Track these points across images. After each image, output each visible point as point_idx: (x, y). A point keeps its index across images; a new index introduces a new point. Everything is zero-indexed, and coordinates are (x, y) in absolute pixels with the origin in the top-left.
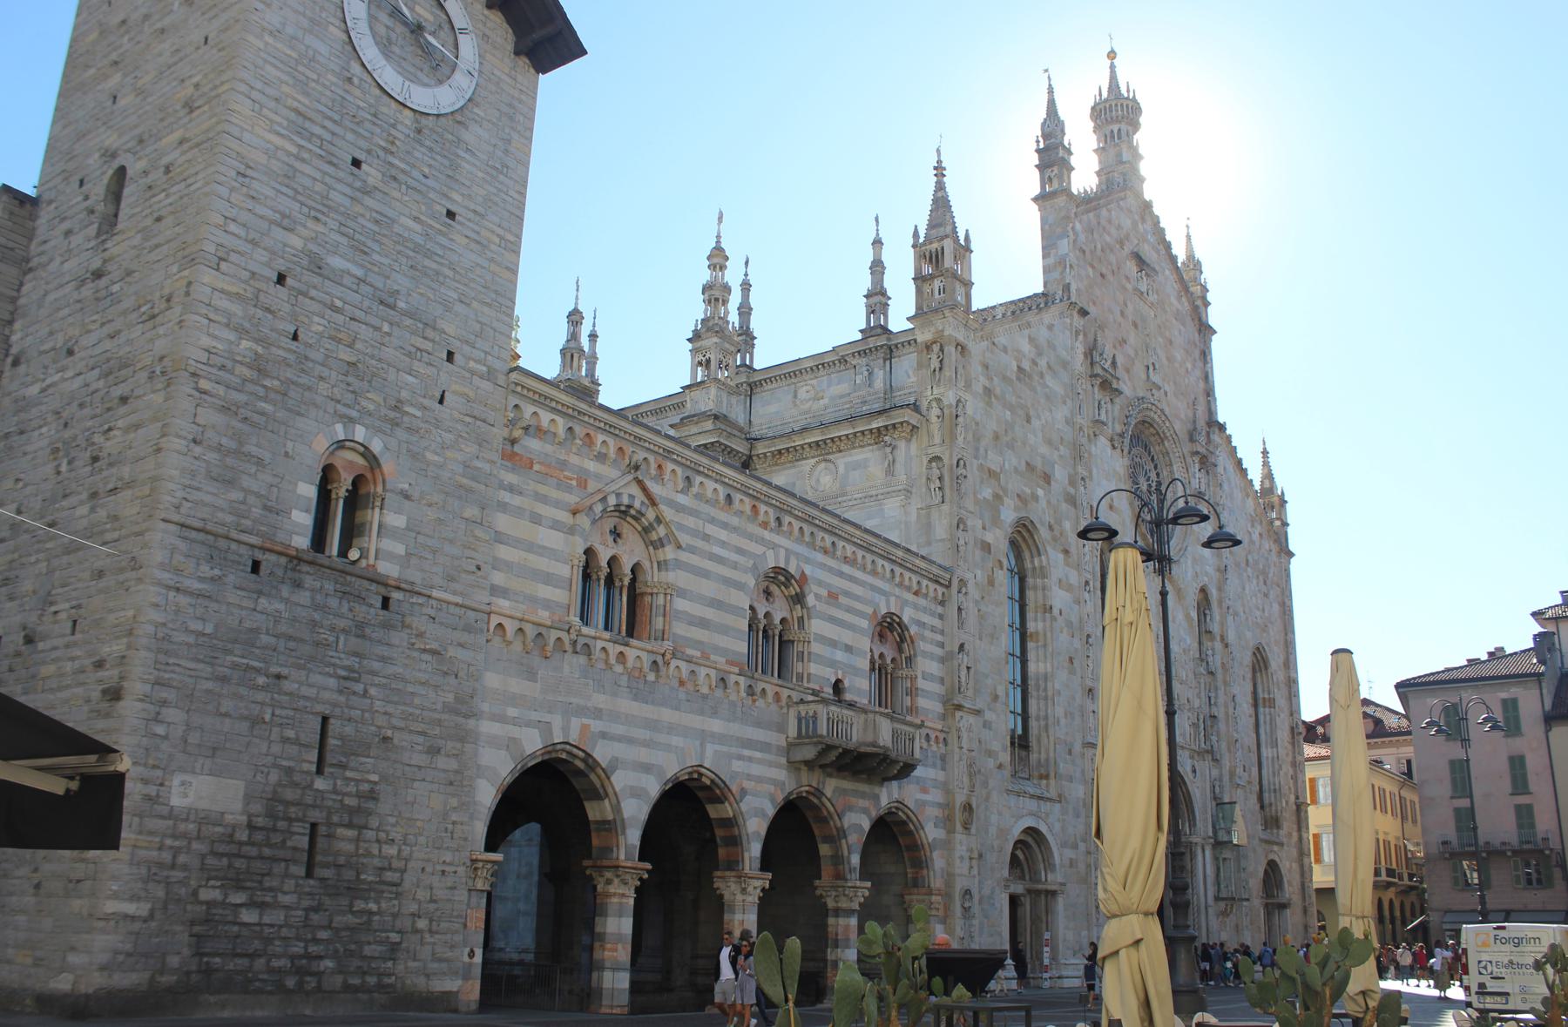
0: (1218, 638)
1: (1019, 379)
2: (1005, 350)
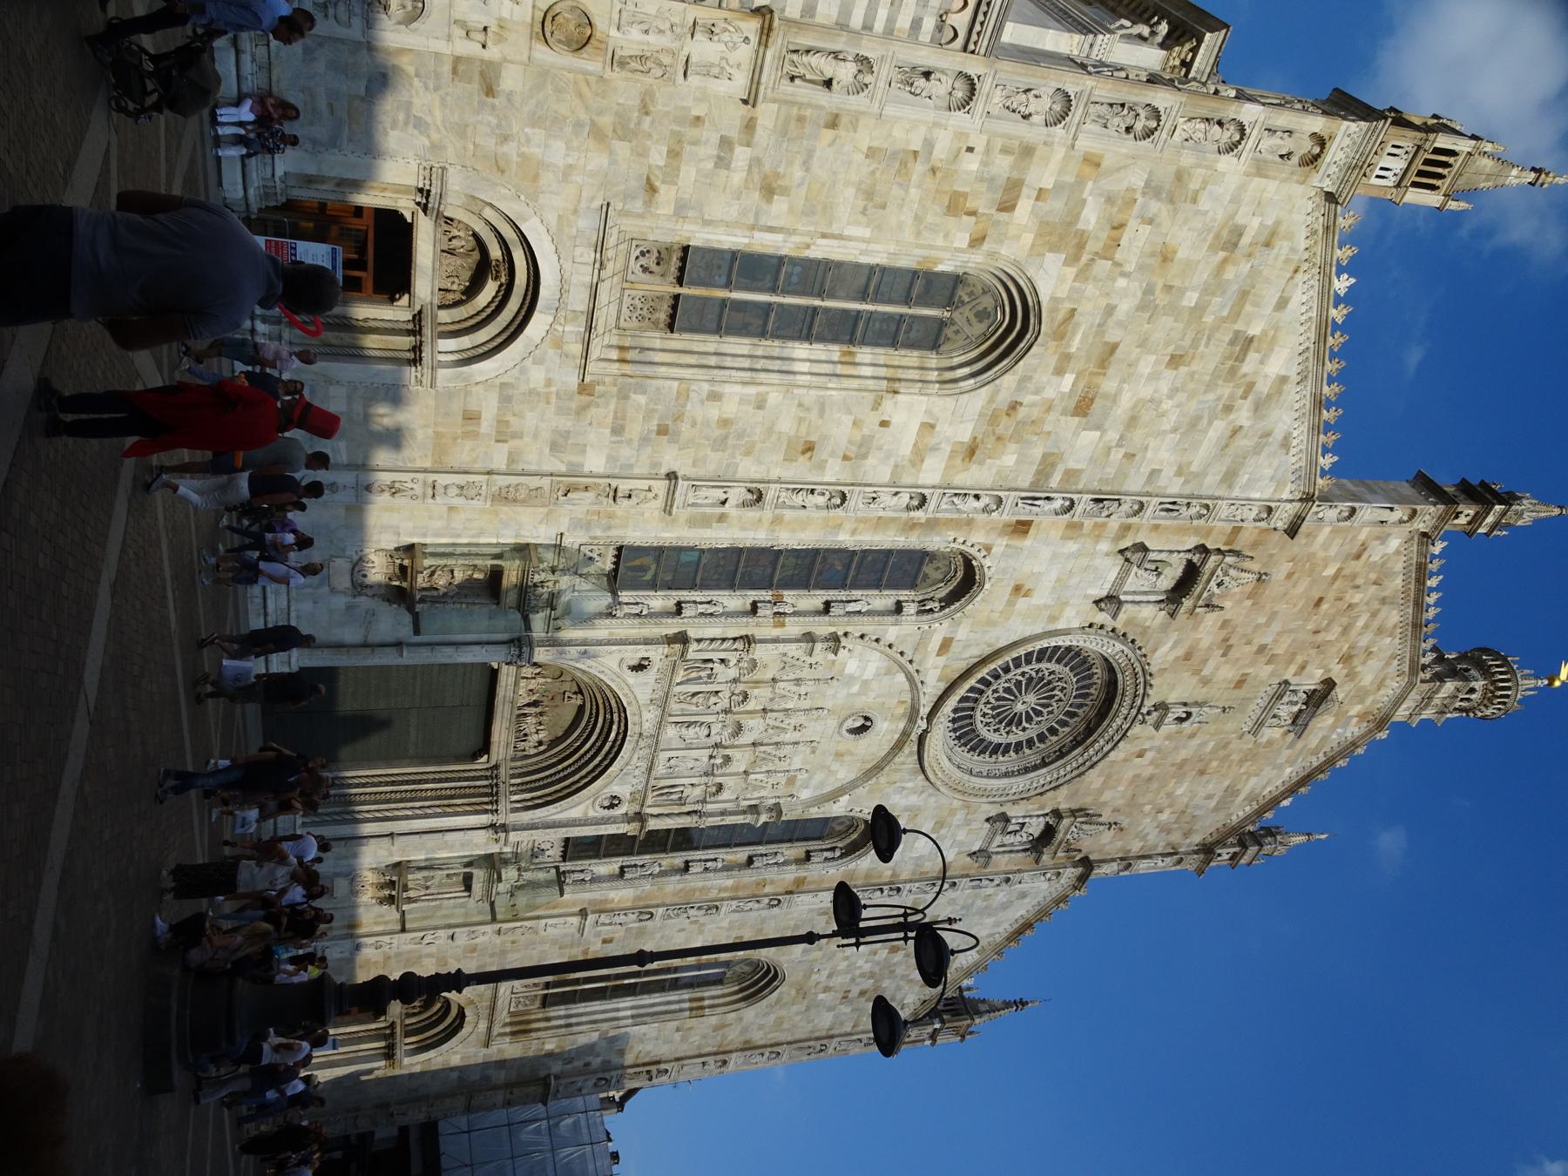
0: (802, 874)
1: (1237, 333)
2: (1282, 304)
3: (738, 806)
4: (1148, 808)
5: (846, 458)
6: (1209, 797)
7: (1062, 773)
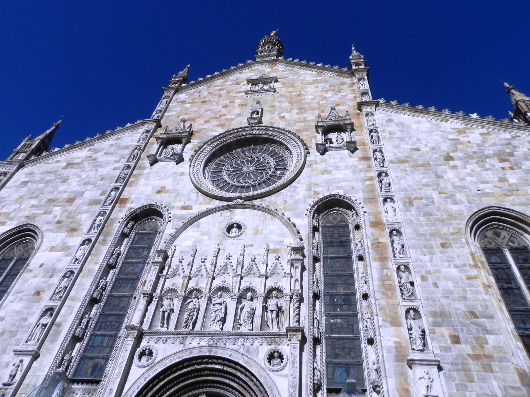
1: (63, 169)
2: (58, 162)
3: (288, 274)
4: (321, 102)
5: (51, 277)
6: (318, 87)
7: (288, 138)
